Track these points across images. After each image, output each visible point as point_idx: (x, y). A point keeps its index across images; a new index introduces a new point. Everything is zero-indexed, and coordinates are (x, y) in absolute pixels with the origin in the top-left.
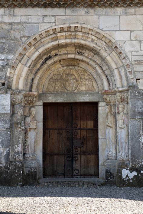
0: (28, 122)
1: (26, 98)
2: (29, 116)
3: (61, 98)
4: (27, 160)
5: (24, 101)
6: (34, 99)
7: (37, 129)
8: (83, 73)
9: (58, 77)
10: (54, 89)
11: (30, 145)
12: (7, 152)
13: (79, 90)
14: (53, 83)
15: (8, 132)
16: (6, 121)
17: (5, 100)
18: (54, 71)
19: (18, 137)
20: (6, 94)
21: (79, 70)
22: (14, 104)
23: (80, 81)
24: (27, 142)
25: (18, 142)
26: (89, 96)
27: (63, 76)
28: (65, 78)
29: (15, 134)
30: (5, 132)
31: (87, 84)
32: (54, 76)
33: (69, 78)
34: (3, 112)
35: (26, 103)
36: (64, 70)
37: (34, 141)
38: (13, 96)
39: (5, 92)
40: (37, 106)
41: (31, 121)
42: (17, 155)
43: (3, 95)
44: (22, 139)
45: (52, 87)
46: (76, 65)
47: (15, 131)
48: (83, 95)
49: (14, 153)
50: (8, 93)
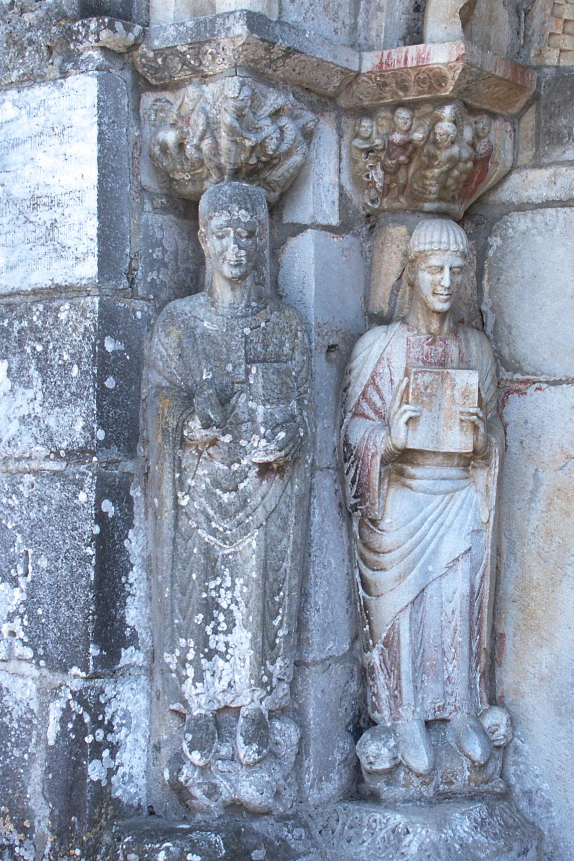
0: (373, 381)
1: (366, 123)
2: (404, 320)
4: (374, 798)
5: (354, 162)
6: (445, 127)
7: (496, 461)
11: (405, 638)
12: (67, 711)
15: (82, 497)
16: (65, 367)
17: (55, 140)
19: (208, 550)
20: (64, 74)
22: (190, 188)
24: (373, 602)
25: (210, 607)
29: (168, 516)
30: (56, 493)
34: (41, 278)
35: (377, 176)
37: (473, 595)
38: (167, 95)
39: (58, 61)
40: (523, 207)
41: (407, 374)
42: (196, 757)
43: (40, 92)
44: (265, 568)
47: (167, 487)
49: (173, 722)
50: (76, 66)
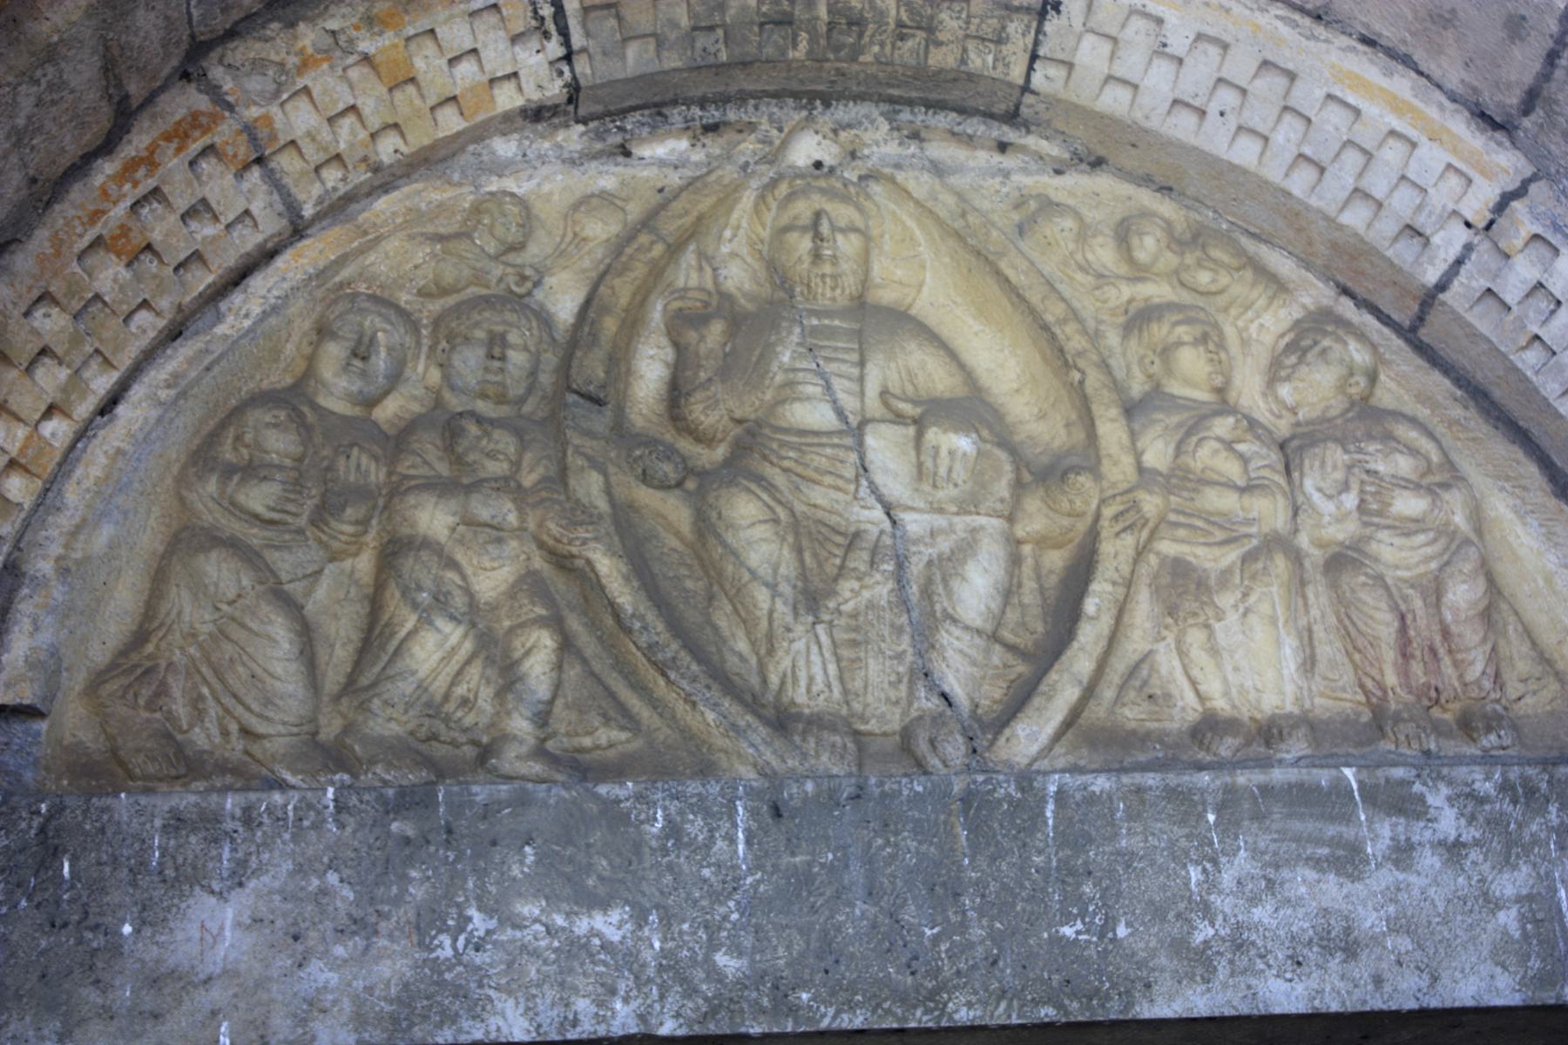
3: (609, 924)
8: (1157, 291)
9: (469, 362)
10: (350, 686)
13: (1133, 714)
14: (324, 513)
18: (338, 207)
21: (1049, 206)
23: (1119, 470)
26: (1511, 850)
27: (620, 363)
28: (676, 392)
31: (1342, 561)
32: (361, 352)
33: (789, 392)
36: (635, 210)
45: (280, 631)
46: (980, 60)
48: (1303, 798)
